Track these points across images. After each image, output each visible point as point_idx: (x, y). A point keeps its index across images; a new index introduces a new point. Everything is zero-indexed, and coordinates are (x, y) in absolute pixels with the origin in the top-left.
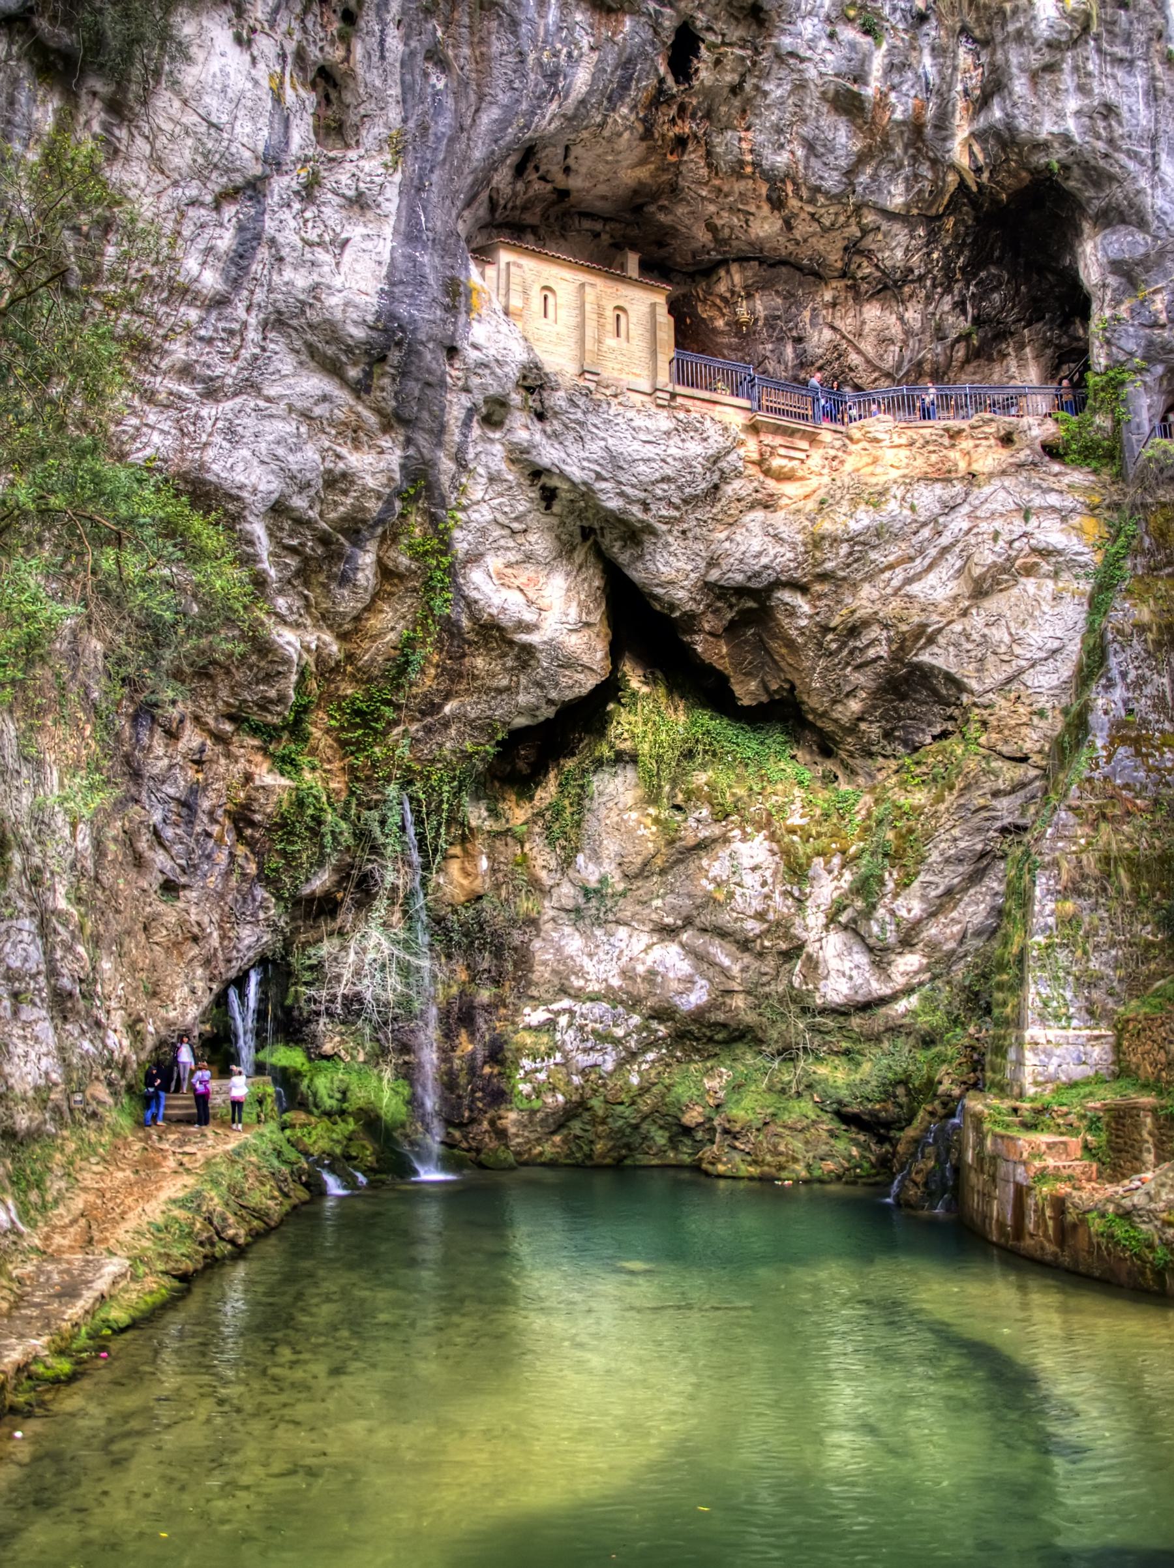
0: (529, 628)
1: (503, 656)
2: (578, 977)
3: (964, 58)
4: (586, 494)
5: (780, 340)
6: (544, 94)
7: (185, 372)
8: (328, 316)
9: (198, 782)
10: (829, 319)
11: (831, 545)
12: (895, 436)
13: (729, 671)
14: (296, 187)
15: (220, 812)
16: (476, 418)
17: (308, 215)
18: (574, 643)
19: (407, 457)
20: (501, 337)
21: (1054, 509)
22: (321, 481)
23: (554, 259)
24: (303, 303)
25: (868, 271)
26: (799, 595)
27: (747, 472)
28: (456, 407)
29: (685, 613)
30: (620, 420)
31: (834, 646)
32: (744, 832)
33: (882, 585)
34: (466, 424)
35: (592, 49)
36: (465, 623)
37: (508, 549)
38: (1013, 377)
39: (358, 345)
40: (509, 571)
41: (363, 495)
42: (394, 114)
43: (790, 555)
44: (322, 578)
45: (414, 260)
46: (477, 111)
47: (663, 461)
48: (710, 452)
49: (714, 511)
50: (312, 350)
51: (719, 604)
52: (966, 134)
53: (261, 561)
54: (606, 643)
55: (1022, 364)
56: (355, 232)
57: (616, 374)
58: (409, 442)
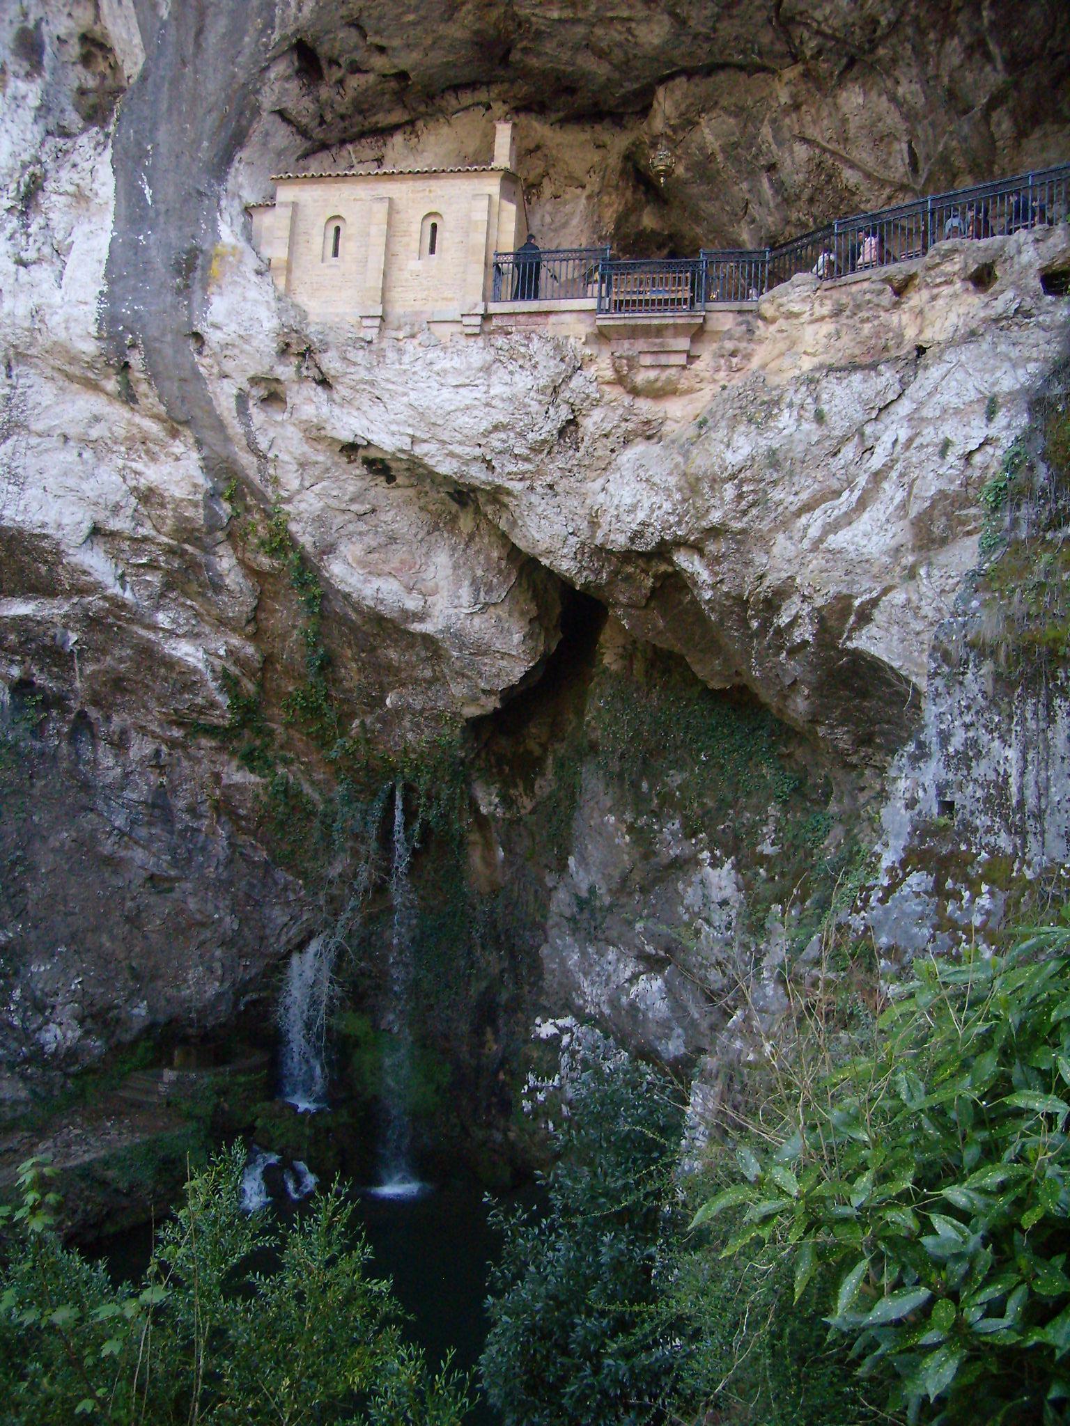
0: (421, 617)
1: (412, 646)
2: (578, 995)
5: (752, 175)
8: (55, 338)
9: (162, 785)
11: (712, 488)
13: (678, 648)
15: (203, 808)
16: (251, 403)
18: (479, 626)
19: (204, 459)
20: (248, 306)
22: (133, 501)
24: (28, 330)
25: (813, 44)
26: (696, 557)
27: (607, 398)
28: (224, 396)
29: (586, 585)
31: (755, 624)
32: (713, 856)
33: (797, 537)
36: (354, 616)
40: (375, 556)
43: (667, 506)
44: (194, 587)
45: (135, 247)
47: (487, 405)
48: (542, 382)
49: (578, 455)
51: (630, 569)
53: (106, 588)
54: (522, 623)
57: (418, 306)
58: (199, 444)
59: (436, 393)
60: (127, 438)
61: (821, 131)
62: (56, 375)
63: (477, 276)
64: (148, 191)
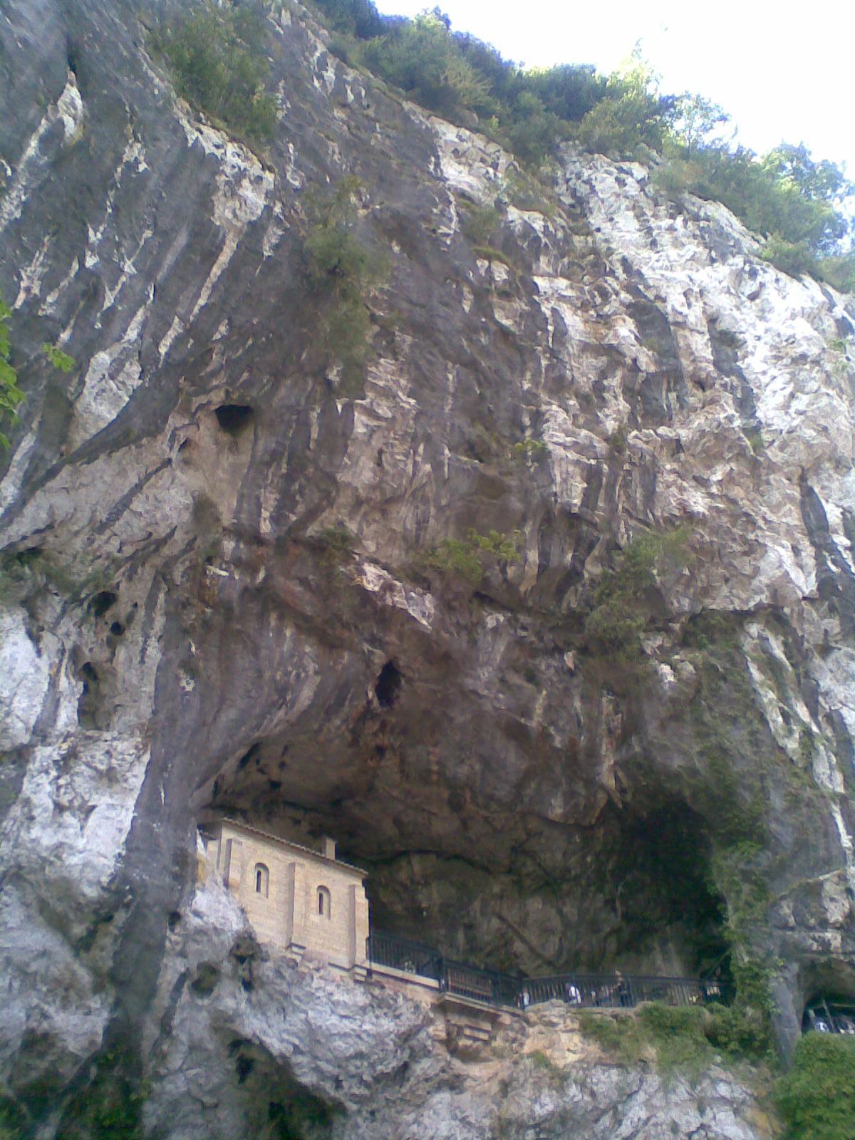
3: (606, 702)
4: (282, 1067)
6: (274, 704)
8: (66, 874)
10: (497, 910)
11: (517, 1132)
12: (568, 1021)
14: (57, 758)
16: (187, 983)
17: (62, 782)
20: (222, 906)
21: (723, 1099)
23: (267, 840)
27: (434, 1052)
30: (320, 994)
34: (177, 989)
35: (316, 673)
37: (195, 1126)
38: (659, 969)
39: (90, 902)
41: (61, 1058)
42: (146, 708)
45: (152, 830)
46: (218, 711)
47: (359, 1036)
48: (403, 1029)
49: (403, 1090)
50: (43, 907)
52: (612, 762)
55: (667, 959)
56: (102, 800)
57: (318, 948)
58: (118, 1003)
59: (328, 1017)
60: (58, 981)
61: (512, 915)
62: (35, 905)
64: (163, 794)
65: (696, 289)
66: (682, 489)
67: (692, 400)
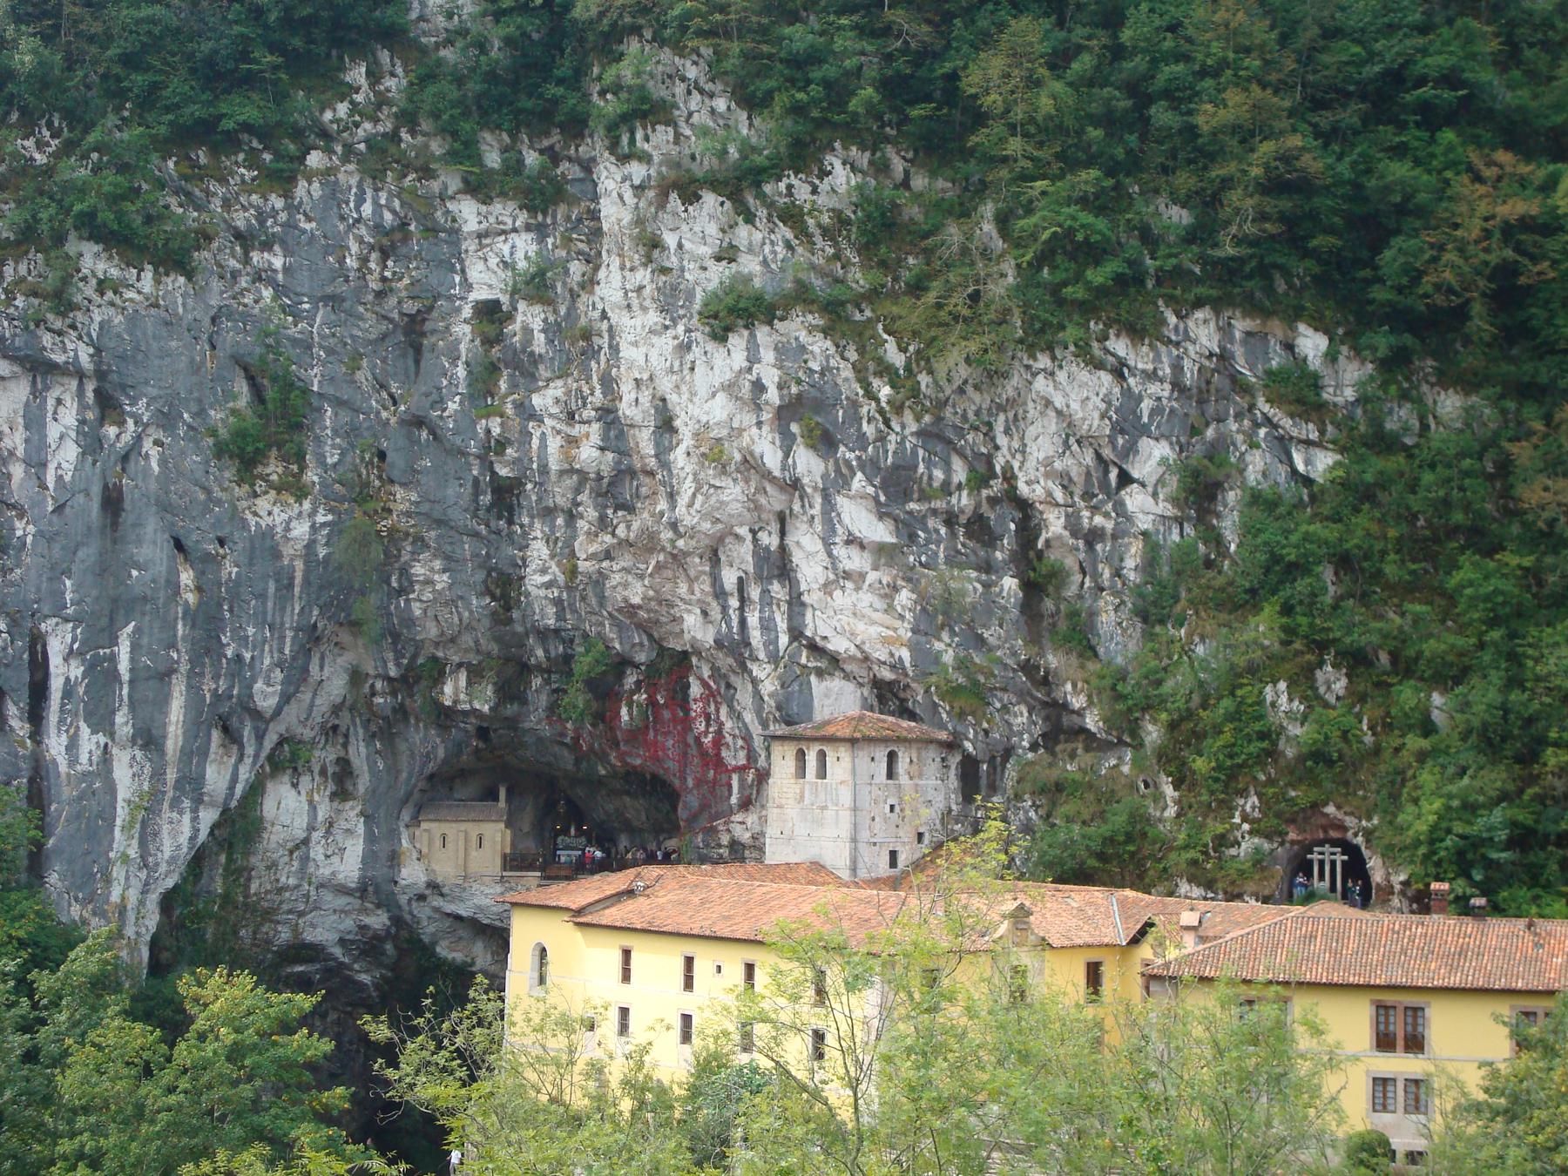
7: (290, 912)
28: (403, 899)
56: (349, 843)
63: (498, 862)
65: (645, 376)
66: (626, 585)
67: (644, 490)
